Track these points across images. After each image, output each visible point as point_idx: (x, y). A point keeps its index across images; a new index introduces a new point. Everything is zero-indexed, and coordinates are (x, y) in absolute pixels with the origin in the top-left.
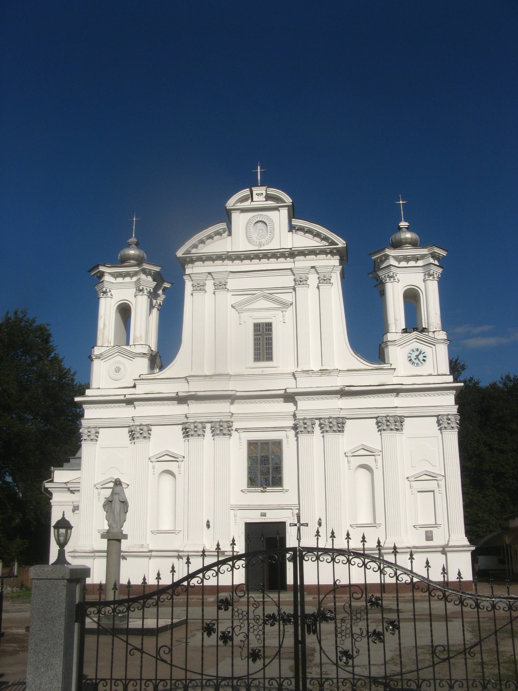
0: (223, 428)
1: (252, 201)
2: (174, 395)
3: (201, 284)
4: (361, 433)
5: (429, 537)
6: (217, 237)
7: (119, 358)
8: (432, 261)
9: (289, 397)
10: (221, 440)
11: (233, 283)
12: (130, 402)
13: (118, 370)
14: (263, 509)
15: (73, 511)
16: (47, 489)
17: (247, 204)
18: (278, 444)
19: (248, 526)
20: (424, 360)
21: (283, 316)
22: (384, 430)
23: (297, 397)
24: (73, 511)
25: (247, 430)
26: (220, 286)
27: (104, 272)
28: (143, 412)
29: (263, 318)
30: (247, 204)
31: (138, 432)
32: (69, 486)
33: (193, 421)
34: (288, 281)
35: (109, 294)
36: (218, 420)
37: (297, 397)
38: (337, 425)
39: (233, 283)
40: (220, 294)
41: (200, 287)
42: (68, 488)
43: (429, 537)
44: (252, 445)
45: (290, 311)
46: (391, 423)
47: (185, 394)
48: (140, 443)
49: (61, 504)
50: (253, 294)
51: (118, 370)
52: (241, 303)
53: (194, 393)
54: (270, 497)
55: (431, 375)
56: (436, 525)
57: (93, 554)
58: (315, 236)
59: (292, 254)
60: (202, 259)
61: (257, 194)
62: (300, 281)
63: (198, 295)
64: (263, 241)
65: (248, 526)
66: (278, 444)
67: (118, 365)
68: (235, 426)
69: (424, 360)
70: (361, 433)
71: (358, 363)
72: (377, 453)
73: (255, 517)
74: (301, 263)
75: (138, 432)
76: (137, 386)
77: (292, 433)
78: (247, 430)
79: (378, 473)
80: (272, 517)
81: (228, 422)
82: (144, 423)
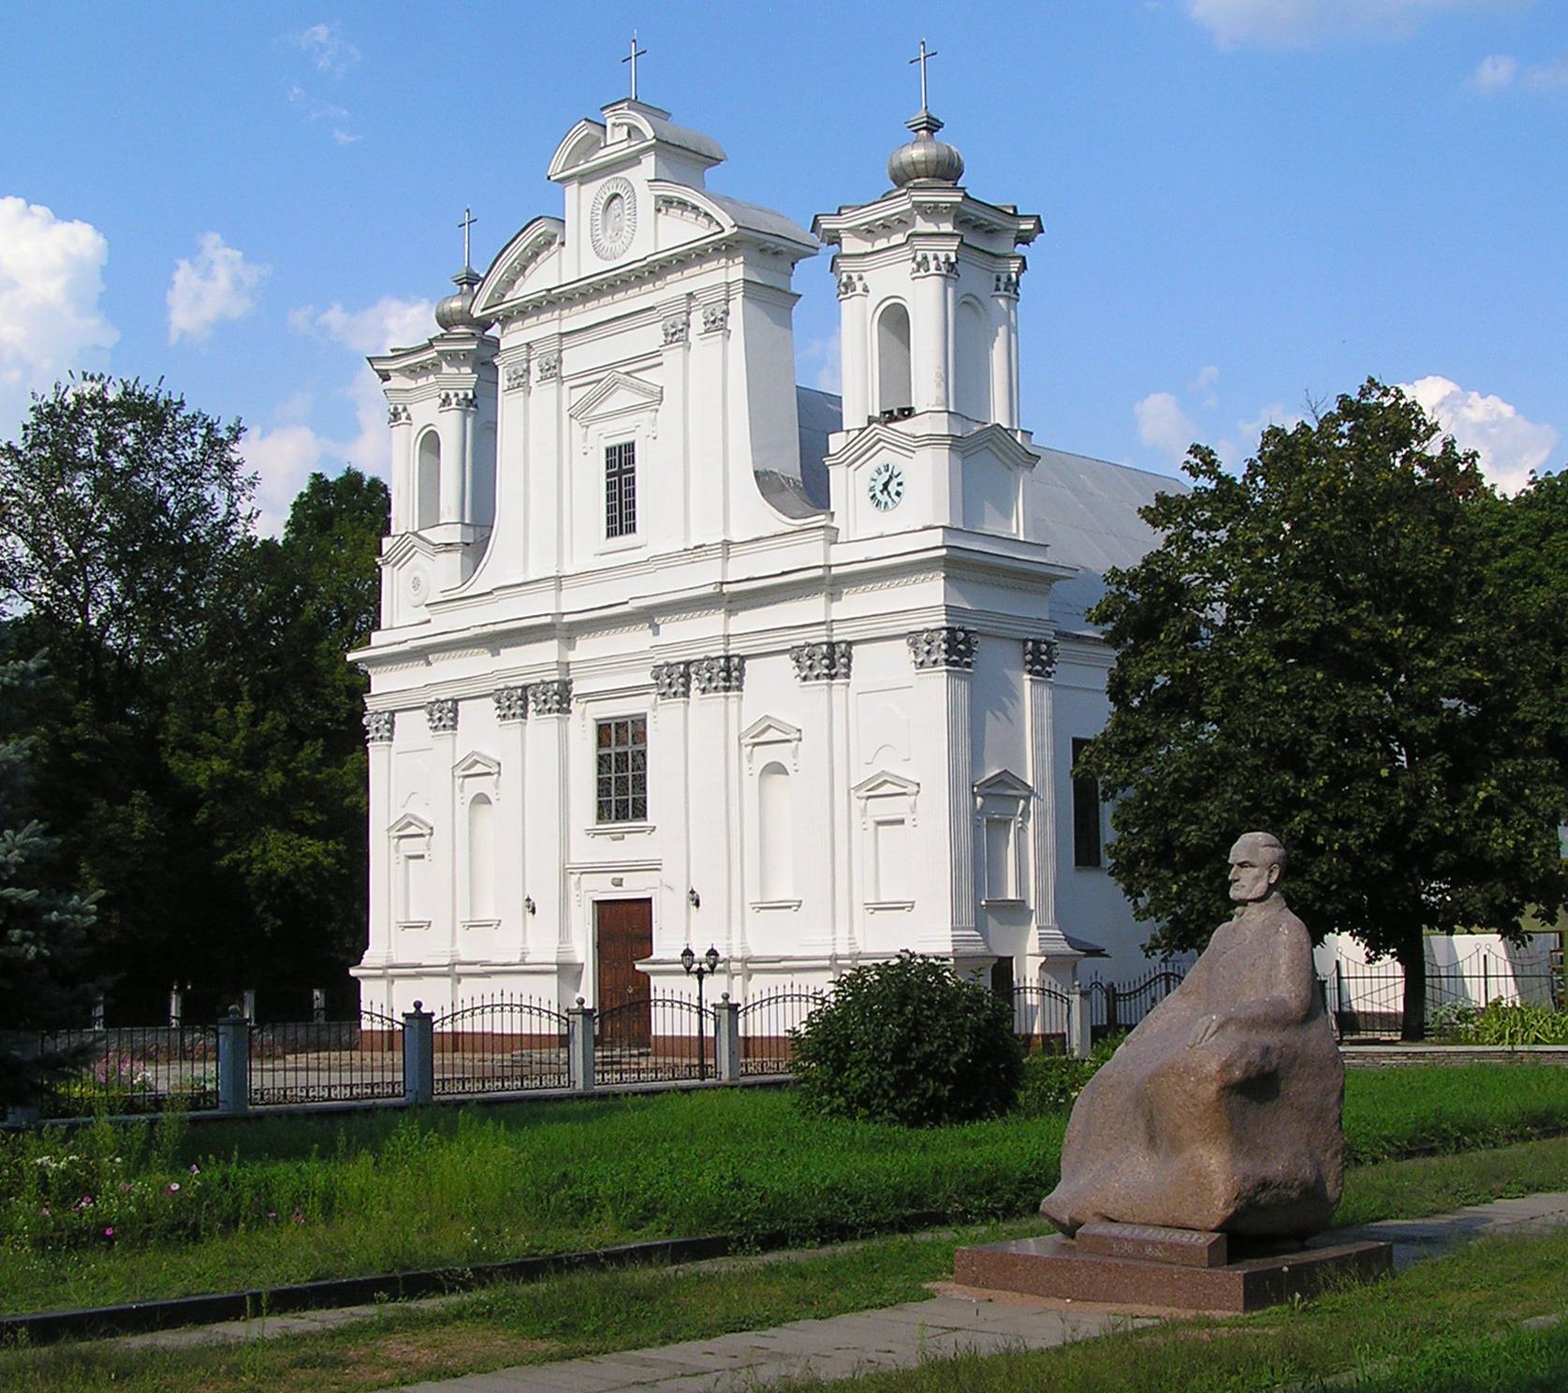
4: (772, 685)
8: (922, 226)
9: (649, 616)
11: (575, 360)
14: (616, 871)
20: (898, 494)
25: (590, 697)
26: (552, 371)
30: (601, 157)
34: (650, 337)
35: (404, 415)
39: (575, 360)
44: (603, 730)
50: (603, 380)
54: (630, 845)
59: (657, 270)
64: (618, 245)
65: (600, 905)
67: (417, 574)
68: (577, 688)
69: (898, 494)
70: (772, 685)
71: (774, 521)
78: (590, 697)
80: (633, 888)
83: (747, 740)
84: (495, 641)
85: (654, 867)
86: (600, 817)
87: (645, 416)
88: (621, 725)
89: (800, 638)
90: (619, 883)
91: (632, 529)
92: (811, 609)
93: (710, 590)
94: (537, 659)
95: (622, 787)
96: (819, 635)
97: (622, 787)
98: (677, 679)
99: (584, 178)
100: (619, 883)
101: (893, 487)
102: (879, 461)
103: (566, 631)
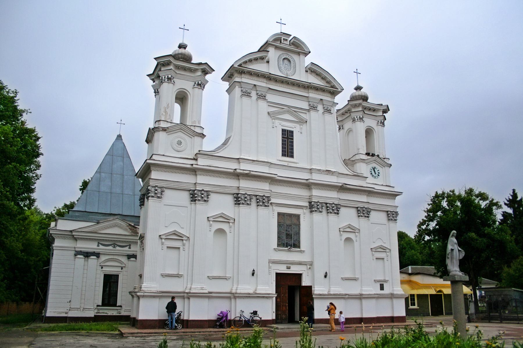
0: (263, 201)
1: (281, 42)
2: (232, 171)
3: (249, 91)
4: (348, 216)
5: (382, 288)
6: (259, 61)
7: (180, 134)
9: (308, 185)
10: (262, 210)
12: (194, 171)
13: (180, 143)
14: (289, 264)
15: (75, 255)
16: (51, 234)
17: (277, 44)
18: (298, 217)
19: (278, 275)
21: (301, 129)
22: (362, 216)
23: (313, 187)
24: (75, 255)
26: (262, 97)
27: (171, 62)
28: (203, 181)
29: (289, 126)
30: (277, 44)
31: (196, 196)
32: (73, 234)
33: (244, 193)
36: (262, 195)
37: (313, 187)
38: (334, 209)
40: (262, 104)
41: (246, 94)
42: (73, 236)
43: (382, 288)
45: (304, 126)
46: (364, 212)
47: (242, 171)
48: (200, 206)
49: (62, 249)
51: (180, 143)
52: (274, 113)
53: (249, 172)
54: (292, 256)
55: (382, 185)
56: (386, 281)
57: (161, 294)
58: (322, 78)
59: (308, 87)
60: (251, 73)
61: (284, 39)
62: (313, 108)
63: (245, 99)
65: (278, 275)
66: (298, 217)
67: (180, 139)
70: (348, 216)
72: (357, 231)
73: (283, 269)
74: (313, 95)
75: (196, 196)
76: (199, 159)
77: (307, 211)
79: (356, 244)
80: (295, 270)
81: (268, 197)
82: (205, 190)
83: (342, 230)
84: (237, 175)
85: (310, 265)
86: (279, 245)
87: (297, 126)
88: (290, 215)
89: (361, 205)
90: (289, 268)
91: (292, 156)
92: (363, 198)
93: (341, 185)
94: (263, 187)
95: (289, 235)
96: (366, 206)
97: (289, 235)
98: (312, 207)
99: (277, 47)
100: (289, 268)
101: (377, 172)
102: (374, 165)
103: (272, 180)
